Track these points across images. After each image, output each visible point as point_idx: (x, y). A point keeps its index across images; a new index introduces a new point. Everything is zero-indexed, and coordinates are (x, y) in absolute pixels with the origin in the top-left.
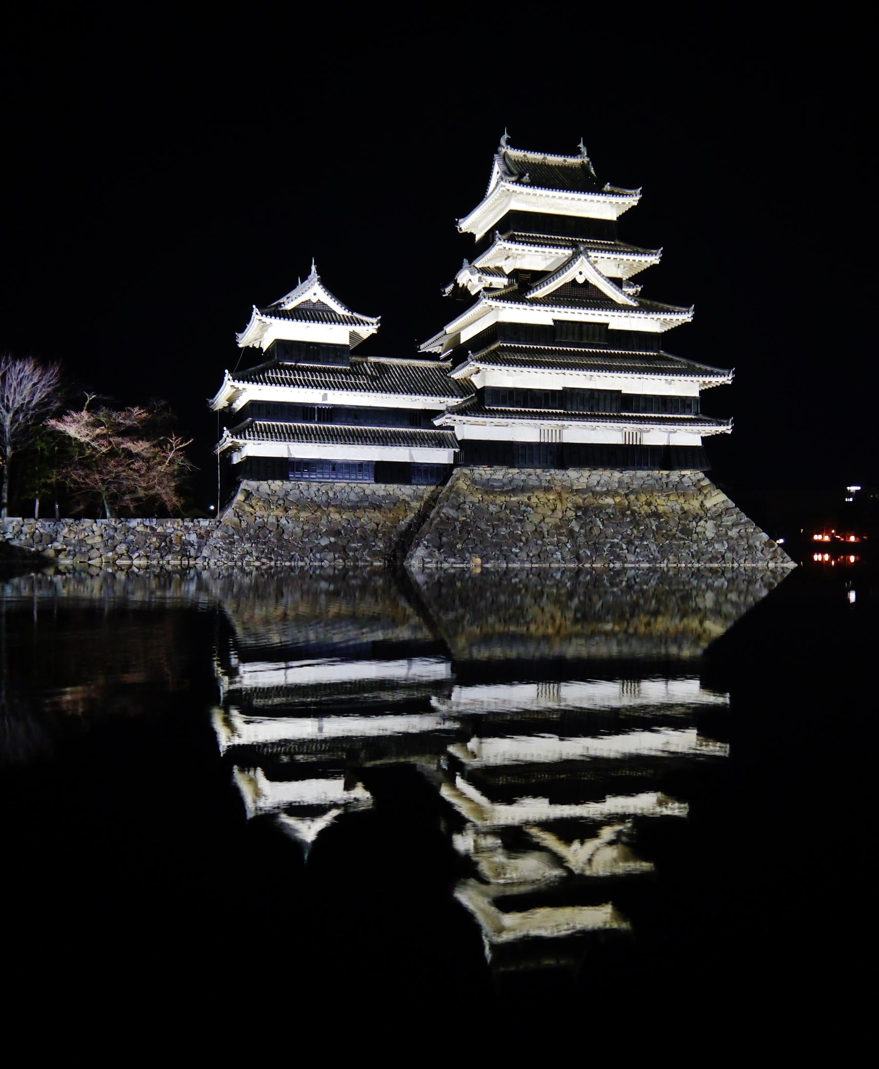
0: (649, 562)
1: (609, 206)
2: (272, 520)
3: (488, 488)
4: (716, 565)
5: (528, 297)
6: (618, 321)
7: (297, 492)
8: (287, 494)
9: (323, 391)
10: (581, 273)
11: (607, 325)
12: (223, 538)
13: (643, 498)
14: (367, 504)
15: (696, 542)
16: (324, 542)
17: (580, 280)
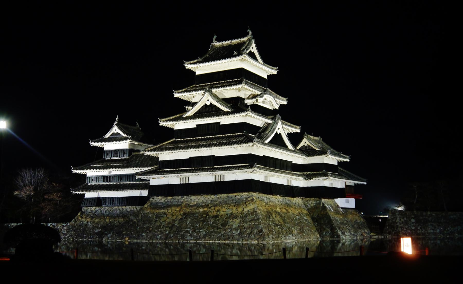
0: (195, 240)
1: (239, 62)
2: (85, 223)
3: (155, 206)
4: (226, 242)
5: (184, 117)
6: (224, 120)
7: (99, 211)
8: (96, 211)
9: (110, 170)
10: (208, 100)
11: (220, 123)
12: (66, 230)
13: (217, 209)
14: (121, 215)
15: (225, 230)
16: (97, 231)
17: (208, 104)
